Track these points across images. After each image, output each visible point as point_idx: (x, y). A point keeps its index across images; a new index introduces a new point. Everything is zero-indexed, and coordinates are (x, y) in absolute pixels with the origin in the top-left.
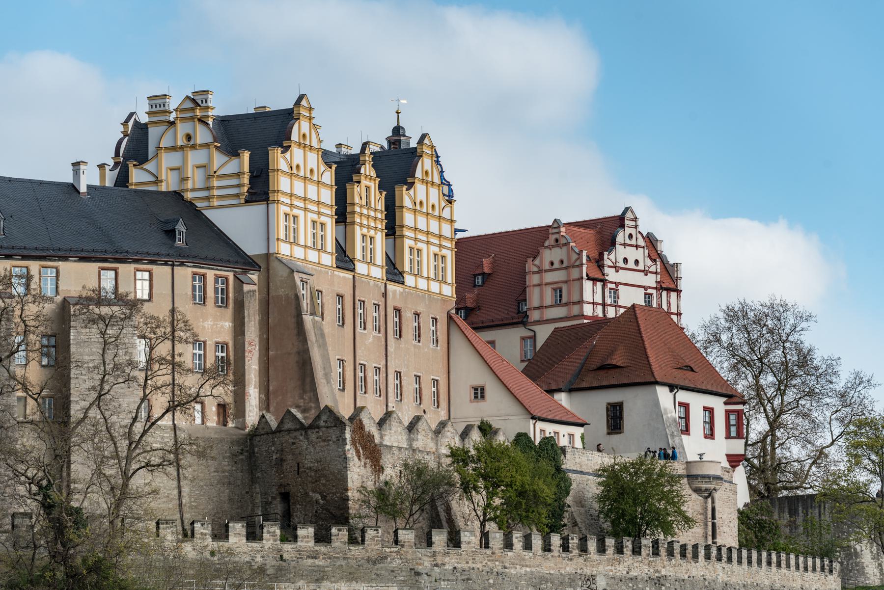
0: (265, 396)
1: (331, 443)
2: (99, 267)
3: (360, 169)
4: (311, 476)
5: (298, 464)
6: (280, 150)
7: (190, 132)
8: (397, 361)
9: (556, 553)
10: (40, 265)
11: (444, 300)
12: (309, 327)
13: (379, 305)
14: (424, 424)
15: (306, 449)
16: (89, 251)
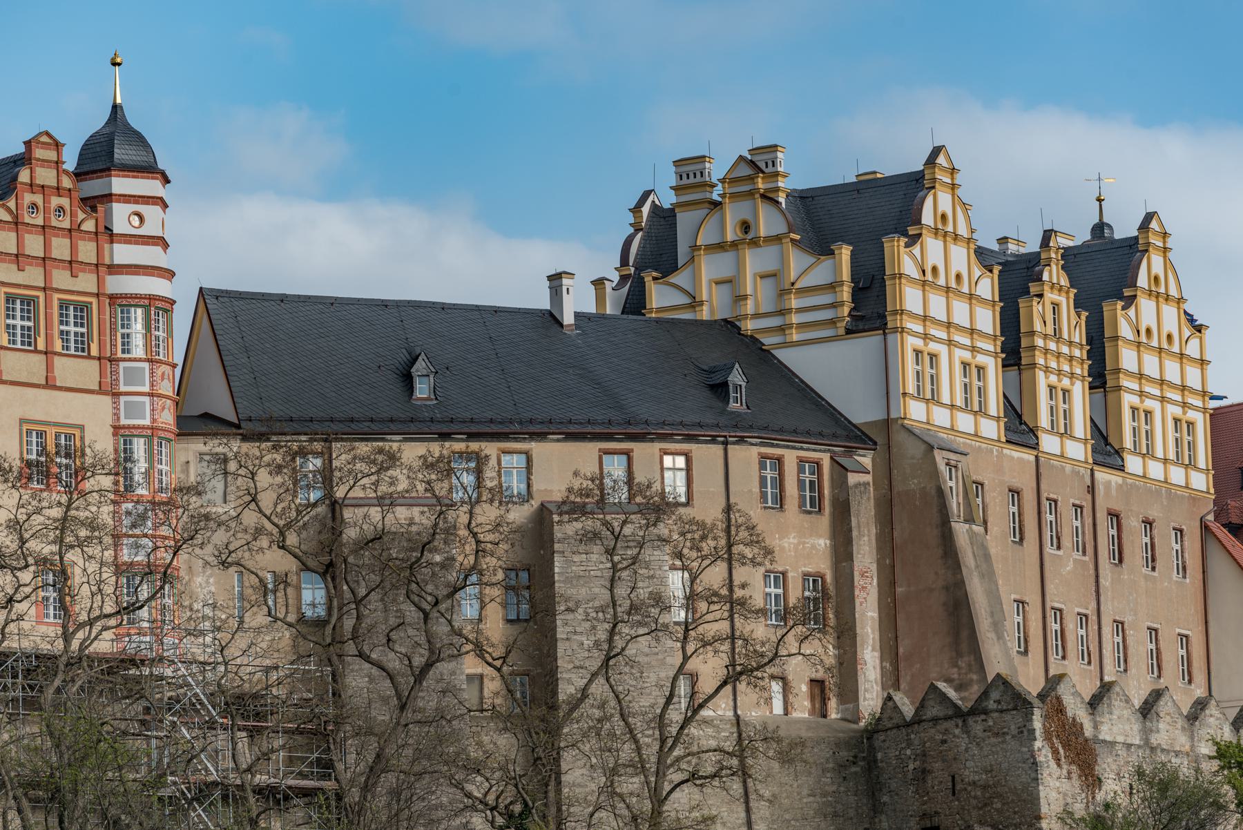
0: (891, 665)
1: (1008, 737)
2: (600, 450)
3: (1041, 273)
4: (975, 797)
5: (953, 777)
6: (903, 240)
7: (749, 217)
8: (1116, 604)
10: (499, 449)
11: (1194, 499)
12: (963, 543)
13: (1081, 507)
14: (1169, 704)
15: (967, 750)
16: (581, 423)
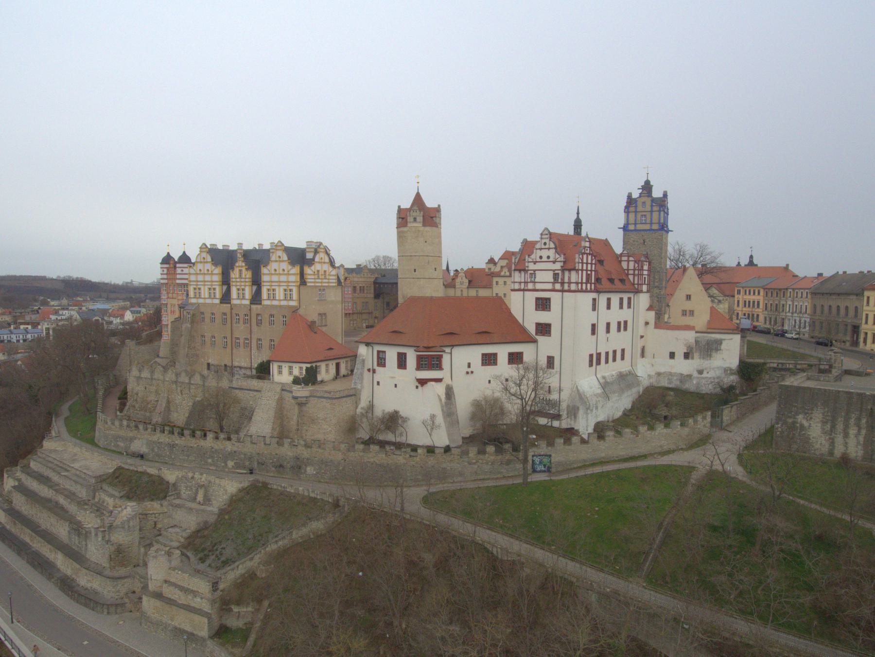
9: (125, 428)
